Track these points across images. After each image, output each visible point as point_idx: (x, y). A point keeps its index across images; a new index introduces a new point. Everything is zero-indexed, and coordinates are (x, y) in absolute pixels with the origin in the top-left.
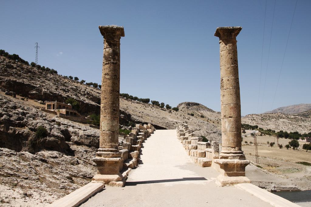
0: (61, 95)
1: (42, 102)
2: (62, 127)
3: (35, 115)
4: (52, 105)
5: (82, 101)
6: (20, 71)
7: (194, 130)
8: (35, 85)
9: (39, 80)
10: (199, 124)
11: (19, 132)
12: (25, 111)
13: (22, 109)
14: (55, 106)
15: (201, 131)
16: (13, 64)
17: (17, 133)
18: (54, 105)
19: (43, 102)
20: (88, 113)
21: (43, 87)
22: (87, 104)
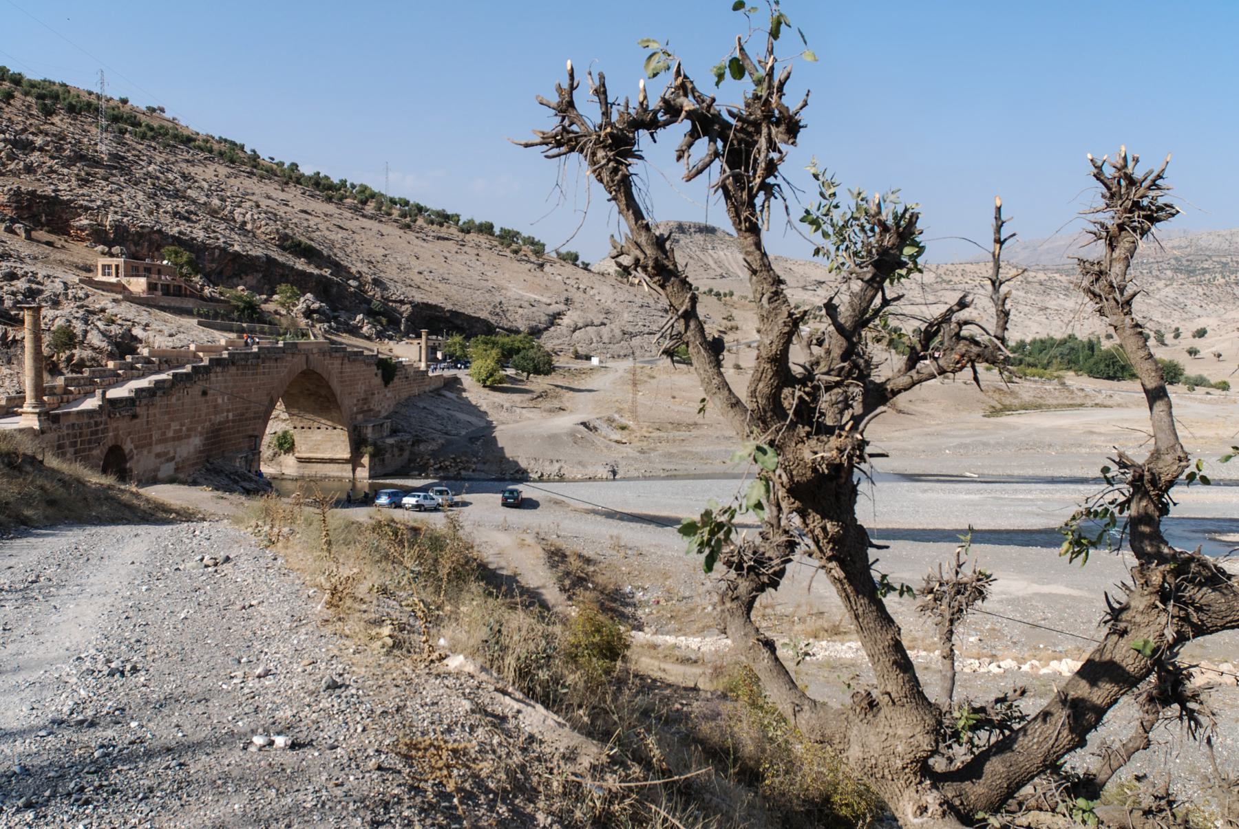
0: (160, 231)
1: (107, 249)
2: (115, 330)
3: (57, 296)
4: (114, 267)
5: (223, 245)
6: (52, 157)
7: (580, 325)
8: (85, 203)
9: (104, 183)
10: (613, 306)
11: (14, 336)
12: (34, 286)
13: (29, 281)
14: (121, 270)
15: (605, 331)
16: (33, 133)
17: (10, 338)
18: (117, 267)
19: (110, 249)
20: (241, 279)
21: (111, 205)
22: (237, 255)
